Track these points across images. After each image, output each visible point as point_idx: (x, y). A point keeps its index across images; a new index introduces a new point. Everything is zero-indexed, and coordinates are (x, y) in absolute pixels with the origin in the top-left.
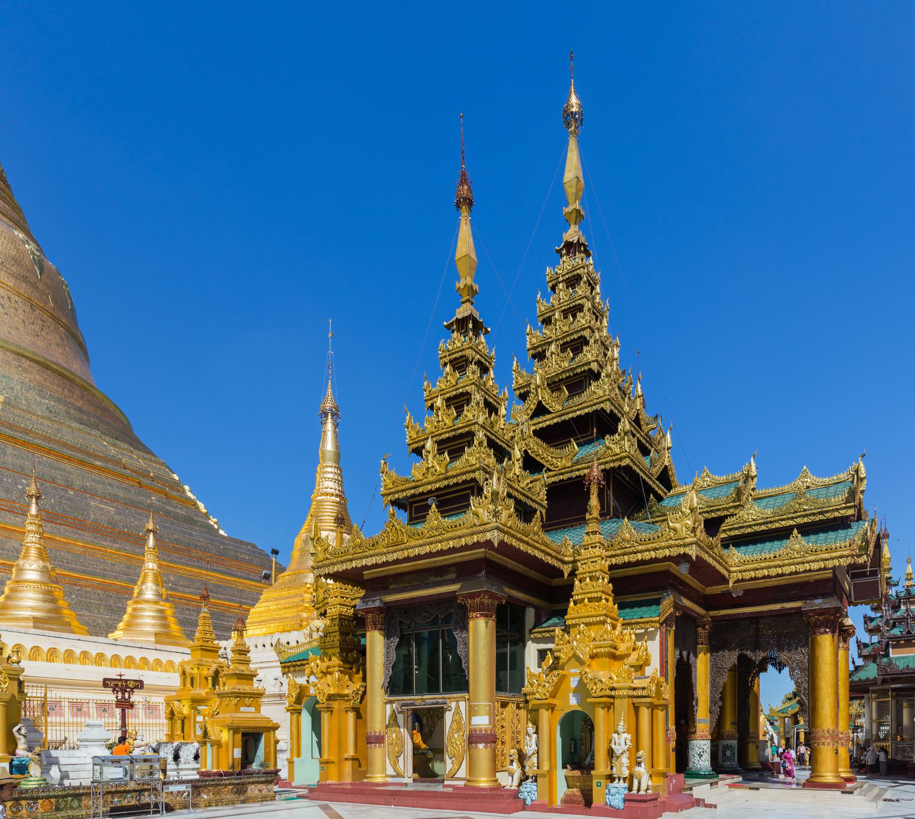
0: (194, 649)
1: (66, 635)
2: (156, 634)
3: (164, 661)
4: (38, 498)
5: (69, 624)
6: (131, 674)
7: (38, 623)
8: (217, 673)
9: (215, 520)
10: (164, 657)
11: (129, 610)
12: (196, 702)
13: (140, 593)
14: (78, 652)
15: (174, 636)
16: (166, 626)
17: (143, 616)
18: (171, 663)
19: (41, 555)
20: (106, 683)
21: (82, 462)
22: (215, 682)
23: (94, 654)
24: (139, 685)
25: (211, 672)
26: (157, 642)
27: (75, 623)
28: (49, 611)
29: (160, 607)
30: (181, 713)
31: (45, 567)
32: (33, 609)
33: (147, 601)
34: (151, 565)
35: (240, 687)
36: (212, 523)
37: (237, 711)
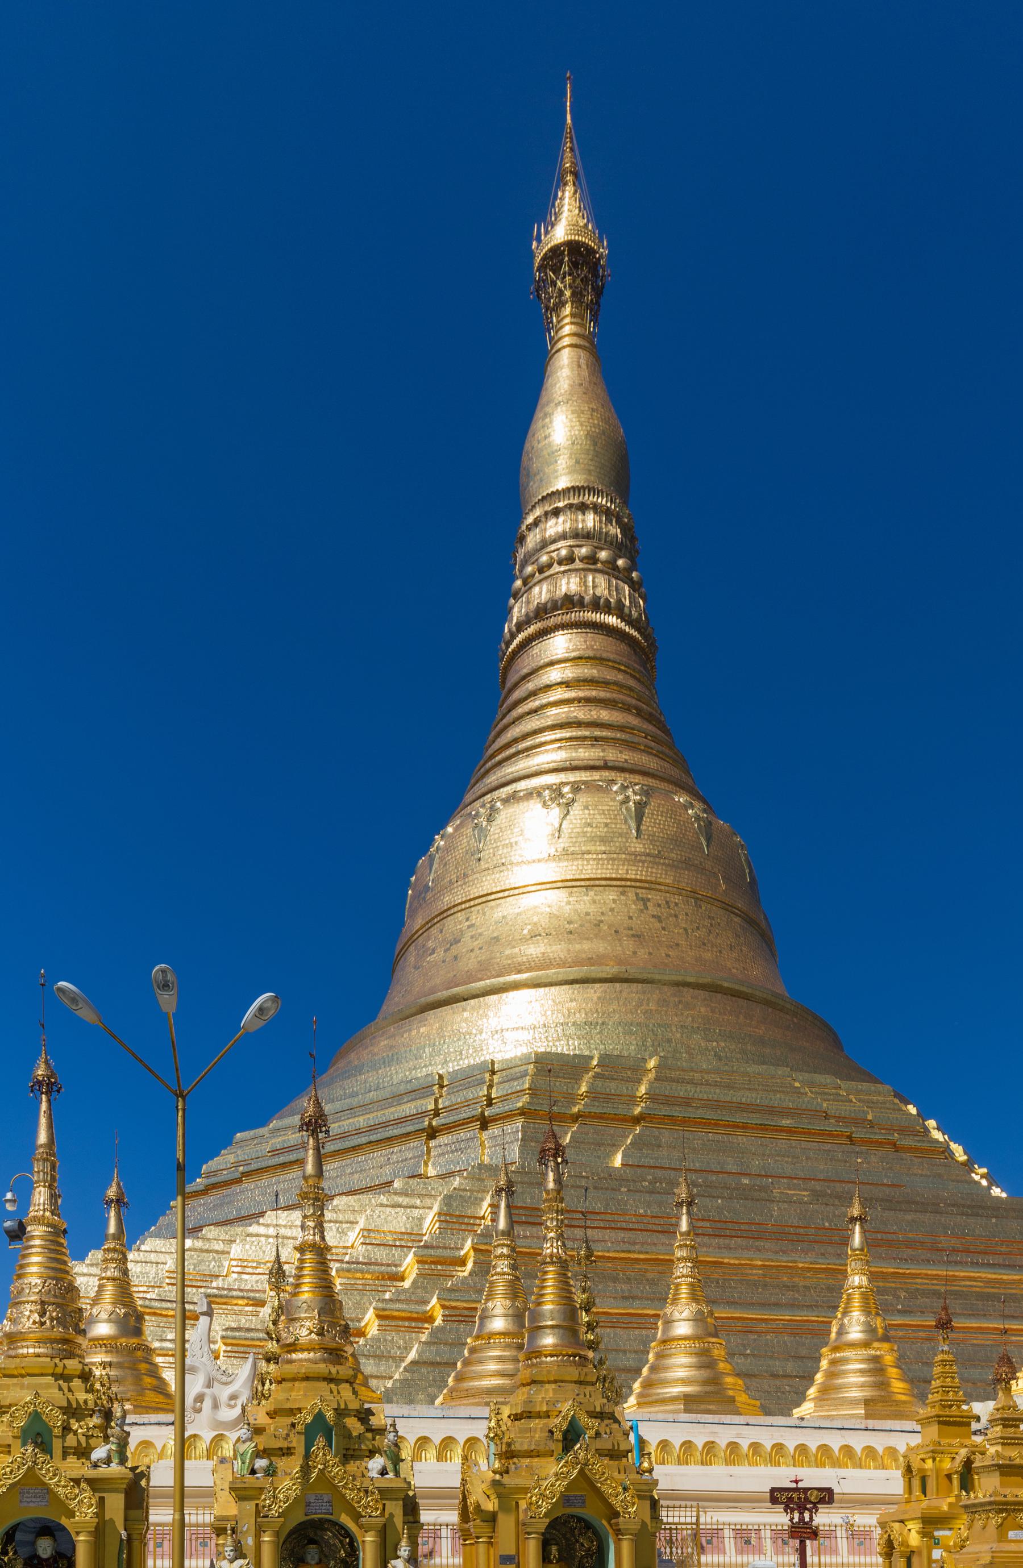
0: (924, 1422)
1: (727, 1419)
2: (867, 1402)
3: (880, 1450)
4: (690, 1204)
5: (732, 1400)
6: (813, 1477)
7: (691, 1403)
8: (968, 1463)
9: (984, 1170)
10: (879, 1442)
11: (824, 1364)
12: (931, 1522)
13: (841, 1332)
14: (744, 1444)
15: (897, 1403)
16: (882, 1385)
17: (845, 1372)
18: (892, 1451)
19: (694, 1297)
20: (776, 1496)
21: (763, 1127)
22: (966, 1481)
23: (768, 1445)
24: (826, 1496)
25: (958, 1465)
26: (868, 1416)
27: (742, 1398)
28: (705, 1382)
29: (873, 1352)
30: (904, 1543)
31: (700, 1312)
32: (684, 1381)
33: (852, 1345)
34: (857, 1280)
35: (1007, 1491)
36: (977, 1178)
37: (1002, 1537)
